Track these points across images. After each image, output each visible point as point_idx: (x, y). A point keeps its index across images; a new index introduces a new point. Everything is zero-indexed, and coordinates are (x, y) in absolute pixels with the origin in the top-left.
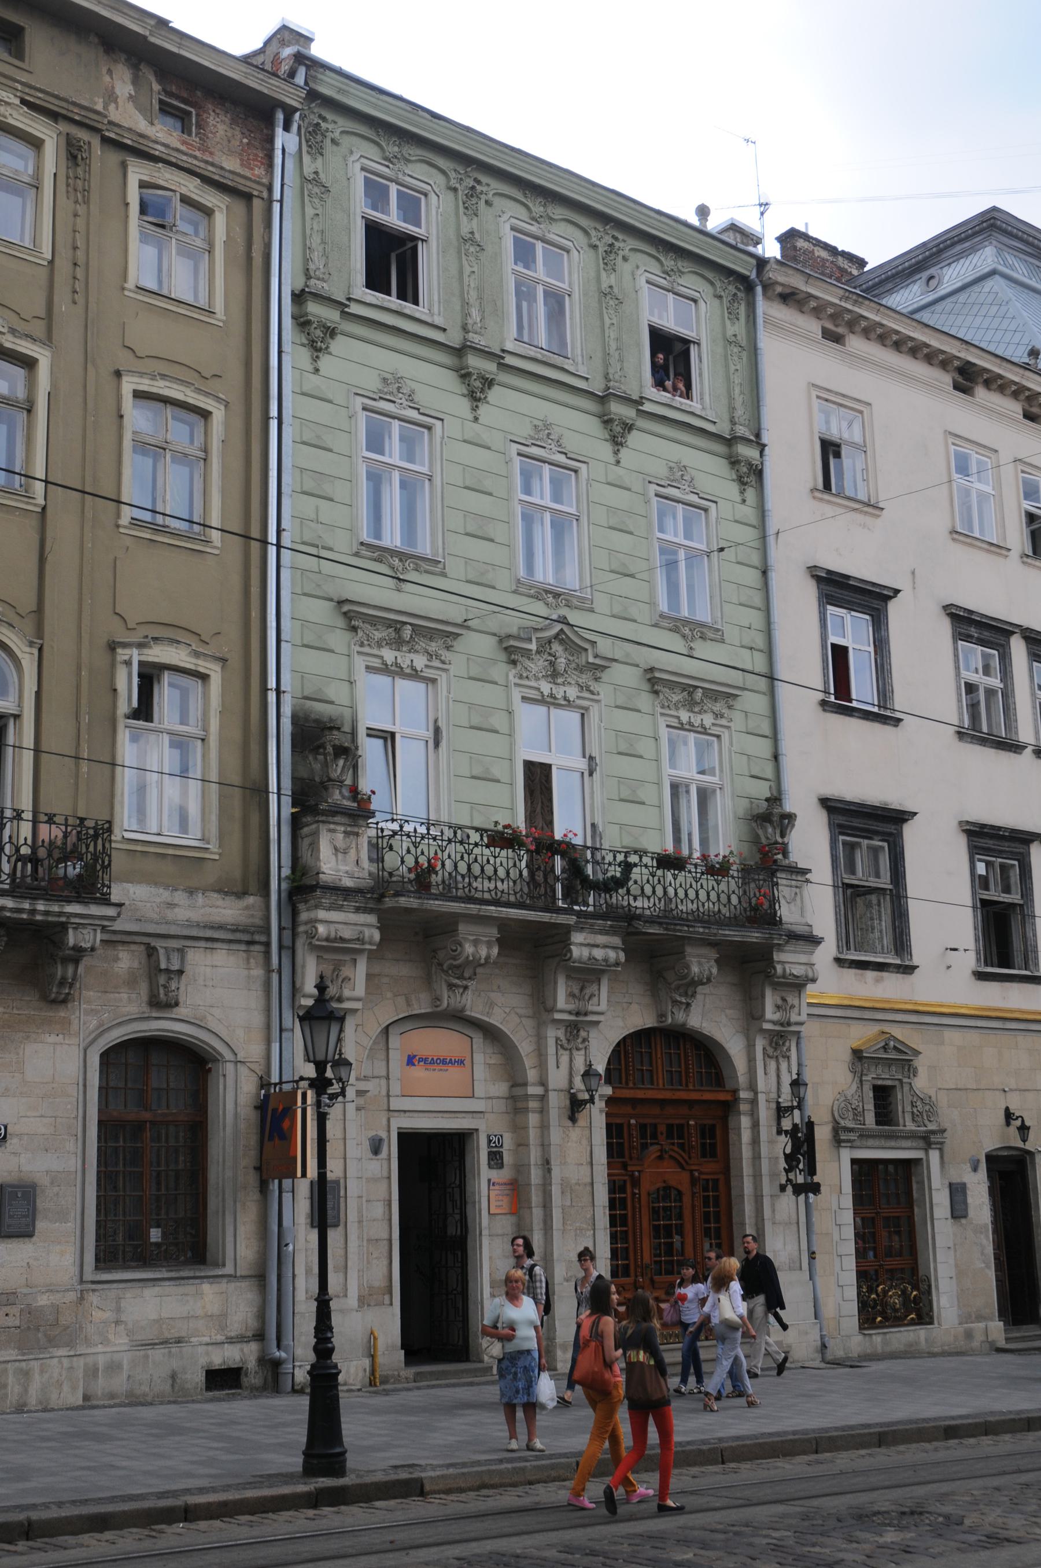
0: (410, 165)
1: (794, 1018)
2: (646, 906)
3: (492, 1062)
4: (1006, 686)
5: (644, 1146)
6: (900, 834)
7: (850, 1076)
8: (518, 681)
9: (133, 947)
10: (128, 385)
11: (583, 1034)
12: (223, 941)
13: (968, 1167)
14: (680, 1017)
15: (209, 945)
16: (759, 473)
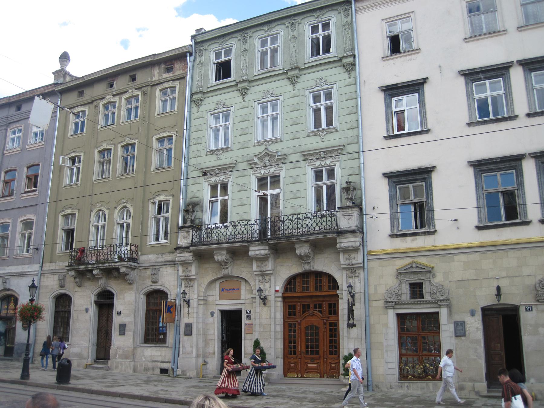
0: (227, 42)
1: (354, 262)
2: (299, 232)
3: (249, 288)
4: (506, 92)
5: (304, 312)
6: (431, 178)
7: (395, 280)
8: (254, 173)
9: (150, 269)
10: (154, 139)
11: (267, 278)
12: (168, 265)
13: (469, 315)
14: (307, 267)
15: (166, 266)
16: (354, 65)
